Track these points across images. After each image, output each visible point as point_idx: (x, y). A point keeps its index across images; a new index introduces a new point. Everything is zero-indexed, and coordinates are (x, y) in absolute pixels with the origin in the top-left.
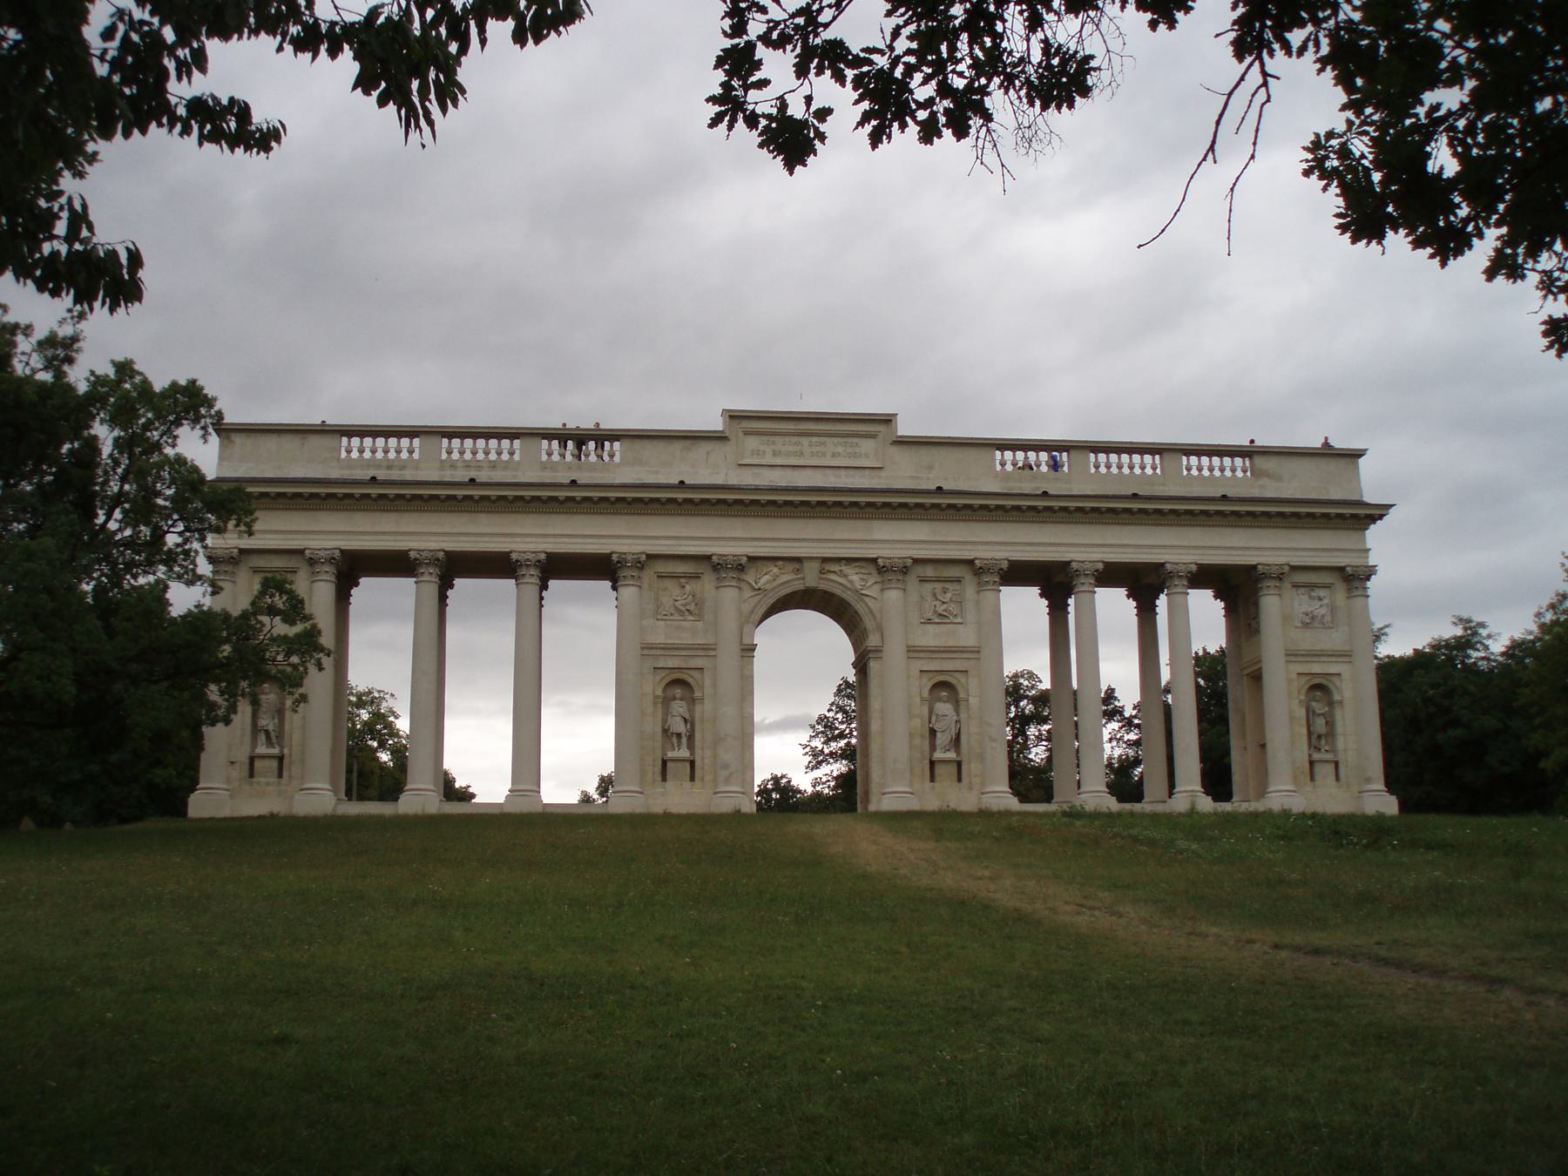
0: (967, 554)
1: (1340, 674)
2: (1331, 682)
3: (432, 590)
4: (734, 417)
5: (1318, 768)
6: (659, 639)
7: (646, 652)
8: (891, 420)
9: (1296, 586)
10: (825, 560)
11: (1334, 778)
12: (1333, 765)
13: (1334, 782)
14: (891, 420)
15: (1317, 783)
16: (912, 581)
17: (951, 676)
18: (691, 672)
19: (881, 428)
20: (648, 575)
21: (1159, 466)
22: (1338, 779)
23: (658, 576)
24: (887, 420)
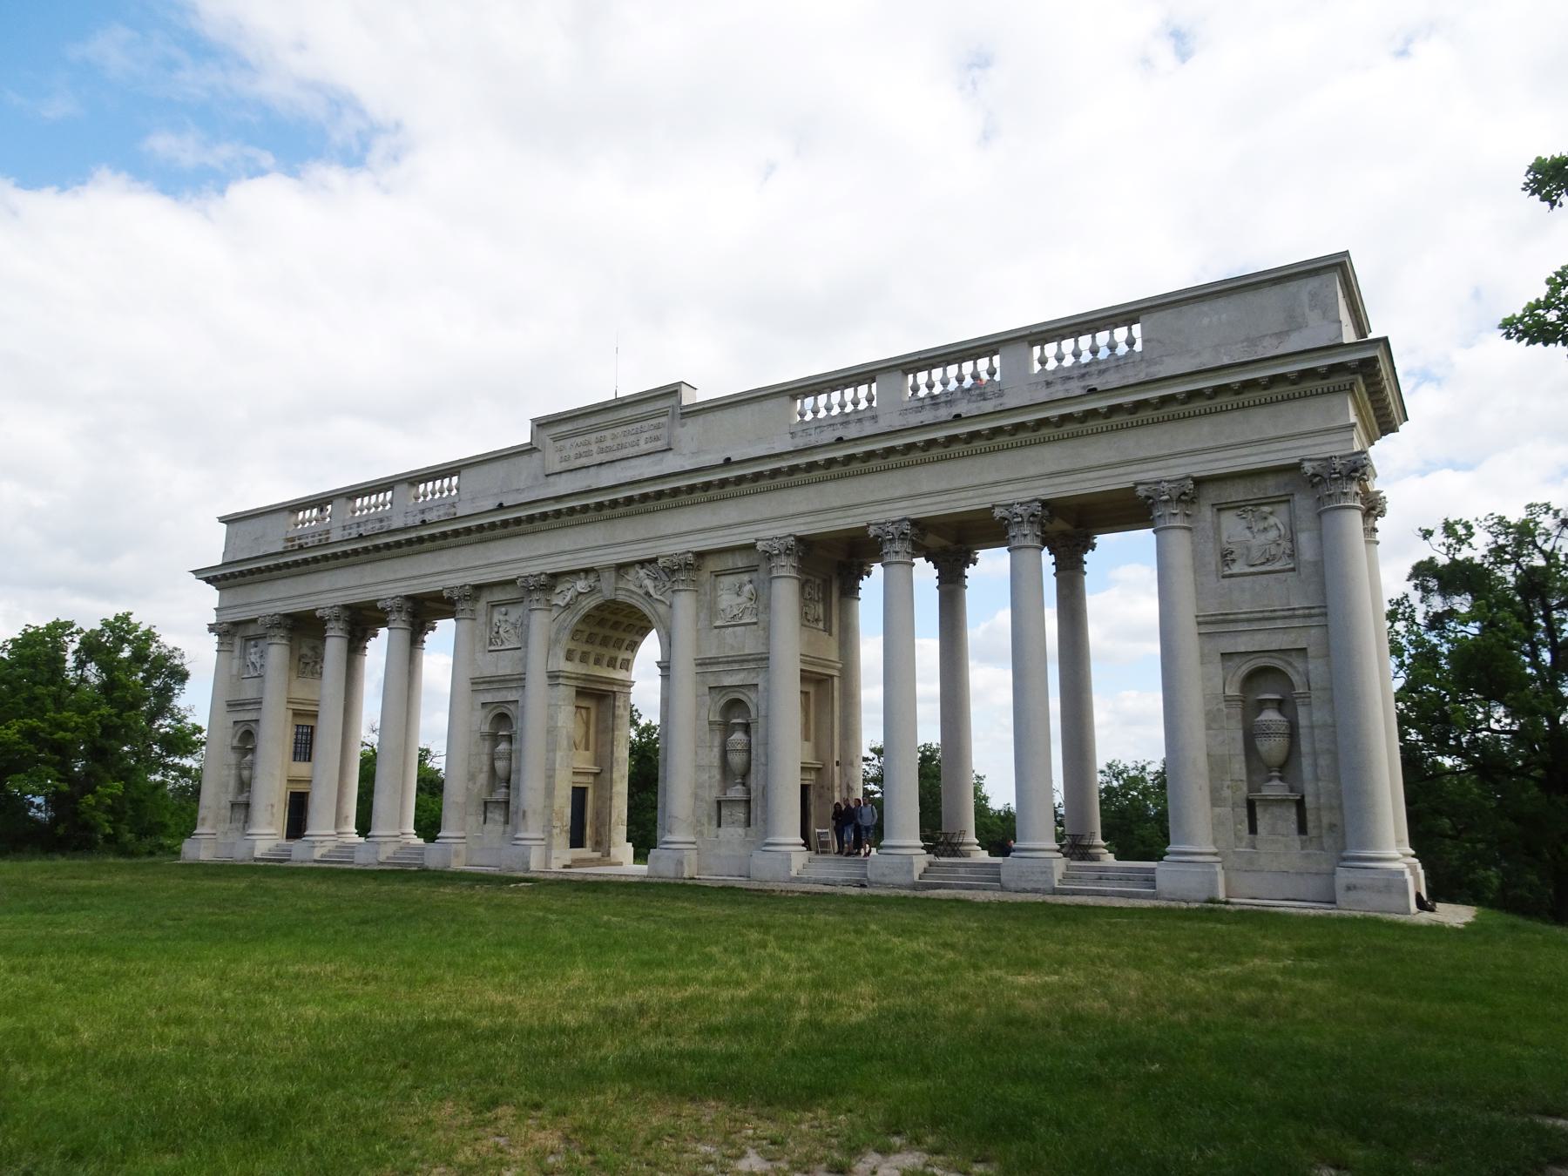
0: (747, 539)
1: (1305, 649)
2: (1290, 664)
3: (403, 636)
4: (541, 424)
5: (1259, 811)
6: (489, 671)
7: (476, 687)
8: (676, 391)
9: (1220, 508)
10: (621, 568)
11: (1294, 826)
12: (1294, 810)
13: (1295, 840)
14: (676, 391)
15: (1258, 836)
16: (705, 576)
17: (743, 693)
18: (512, 707)
19: (671, 402)
20: (482, 605)
21: (998, 370)
22: (1302, 828)
23: (493, 606)
24: (672, 391)
